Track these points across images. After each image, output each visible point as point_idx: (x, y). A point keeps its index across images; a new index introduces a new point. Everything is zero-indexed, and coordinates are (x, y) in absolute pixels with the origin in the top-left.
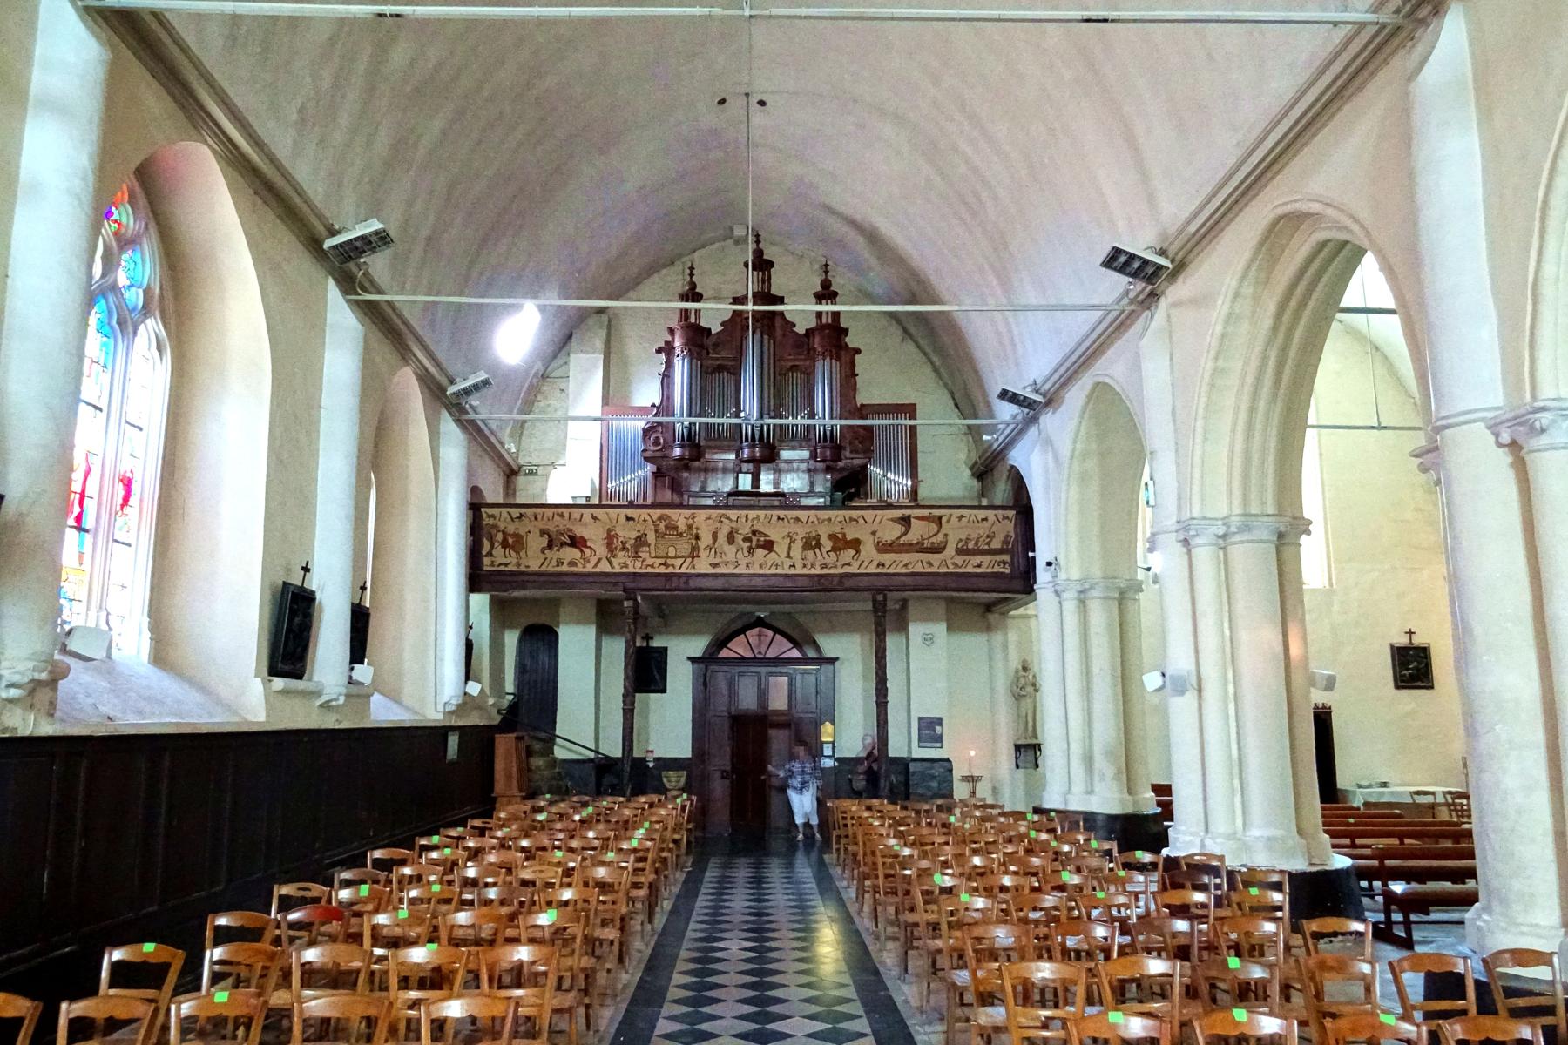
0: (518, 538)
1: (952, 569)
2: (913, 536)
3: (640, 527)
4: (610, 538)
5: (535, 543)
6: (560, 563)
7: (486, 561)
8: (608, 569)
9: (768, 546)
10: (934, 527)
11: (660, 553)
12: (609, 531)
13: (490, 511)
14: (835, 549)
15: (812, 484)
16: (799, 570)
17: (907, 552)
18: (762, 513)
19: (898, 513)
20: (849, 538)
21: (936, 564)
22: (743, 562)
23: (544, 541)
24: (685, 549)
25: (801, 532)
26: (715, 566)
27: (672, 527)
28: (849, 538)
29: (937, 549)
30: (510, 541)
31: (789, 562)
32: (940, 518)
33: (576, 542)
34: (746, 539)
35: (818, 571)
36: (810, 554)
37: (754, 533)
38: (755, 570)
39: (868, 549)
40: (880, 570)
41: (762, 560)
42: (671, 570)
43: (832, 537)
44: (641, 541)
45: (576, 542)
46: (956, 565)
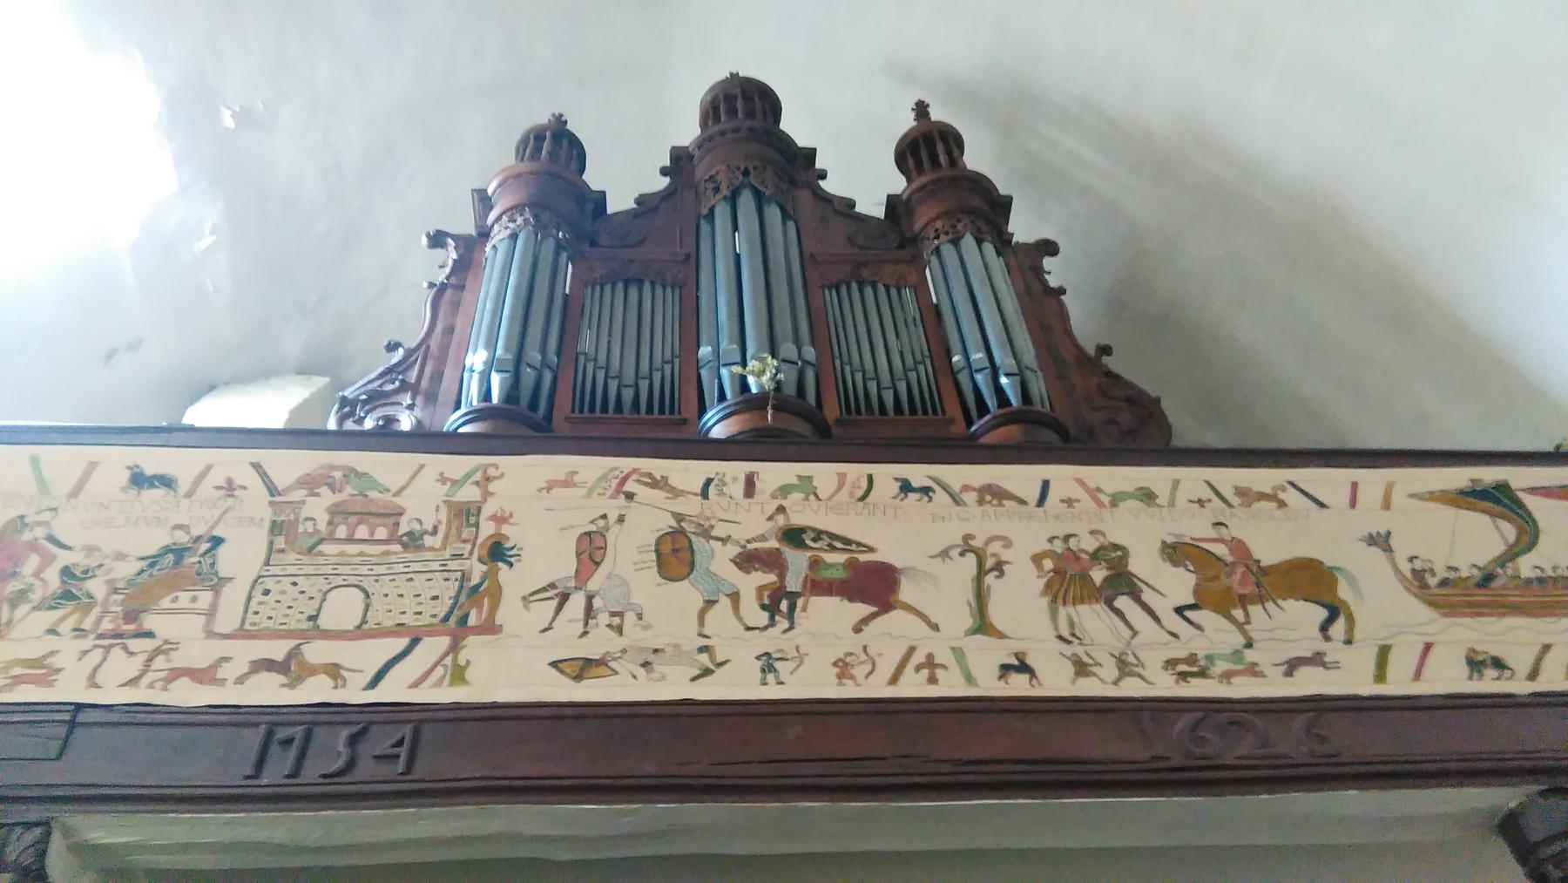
11: (268, 613)
16: (1056, 681)
24: (424, 592)
25: (1026, 537)
26: (584, 668)
34: (747, 561)
35: (1165, 686)
36: (1092, 618)
37: (794, 536)
42: (316, 690)
43: (1176, 552)
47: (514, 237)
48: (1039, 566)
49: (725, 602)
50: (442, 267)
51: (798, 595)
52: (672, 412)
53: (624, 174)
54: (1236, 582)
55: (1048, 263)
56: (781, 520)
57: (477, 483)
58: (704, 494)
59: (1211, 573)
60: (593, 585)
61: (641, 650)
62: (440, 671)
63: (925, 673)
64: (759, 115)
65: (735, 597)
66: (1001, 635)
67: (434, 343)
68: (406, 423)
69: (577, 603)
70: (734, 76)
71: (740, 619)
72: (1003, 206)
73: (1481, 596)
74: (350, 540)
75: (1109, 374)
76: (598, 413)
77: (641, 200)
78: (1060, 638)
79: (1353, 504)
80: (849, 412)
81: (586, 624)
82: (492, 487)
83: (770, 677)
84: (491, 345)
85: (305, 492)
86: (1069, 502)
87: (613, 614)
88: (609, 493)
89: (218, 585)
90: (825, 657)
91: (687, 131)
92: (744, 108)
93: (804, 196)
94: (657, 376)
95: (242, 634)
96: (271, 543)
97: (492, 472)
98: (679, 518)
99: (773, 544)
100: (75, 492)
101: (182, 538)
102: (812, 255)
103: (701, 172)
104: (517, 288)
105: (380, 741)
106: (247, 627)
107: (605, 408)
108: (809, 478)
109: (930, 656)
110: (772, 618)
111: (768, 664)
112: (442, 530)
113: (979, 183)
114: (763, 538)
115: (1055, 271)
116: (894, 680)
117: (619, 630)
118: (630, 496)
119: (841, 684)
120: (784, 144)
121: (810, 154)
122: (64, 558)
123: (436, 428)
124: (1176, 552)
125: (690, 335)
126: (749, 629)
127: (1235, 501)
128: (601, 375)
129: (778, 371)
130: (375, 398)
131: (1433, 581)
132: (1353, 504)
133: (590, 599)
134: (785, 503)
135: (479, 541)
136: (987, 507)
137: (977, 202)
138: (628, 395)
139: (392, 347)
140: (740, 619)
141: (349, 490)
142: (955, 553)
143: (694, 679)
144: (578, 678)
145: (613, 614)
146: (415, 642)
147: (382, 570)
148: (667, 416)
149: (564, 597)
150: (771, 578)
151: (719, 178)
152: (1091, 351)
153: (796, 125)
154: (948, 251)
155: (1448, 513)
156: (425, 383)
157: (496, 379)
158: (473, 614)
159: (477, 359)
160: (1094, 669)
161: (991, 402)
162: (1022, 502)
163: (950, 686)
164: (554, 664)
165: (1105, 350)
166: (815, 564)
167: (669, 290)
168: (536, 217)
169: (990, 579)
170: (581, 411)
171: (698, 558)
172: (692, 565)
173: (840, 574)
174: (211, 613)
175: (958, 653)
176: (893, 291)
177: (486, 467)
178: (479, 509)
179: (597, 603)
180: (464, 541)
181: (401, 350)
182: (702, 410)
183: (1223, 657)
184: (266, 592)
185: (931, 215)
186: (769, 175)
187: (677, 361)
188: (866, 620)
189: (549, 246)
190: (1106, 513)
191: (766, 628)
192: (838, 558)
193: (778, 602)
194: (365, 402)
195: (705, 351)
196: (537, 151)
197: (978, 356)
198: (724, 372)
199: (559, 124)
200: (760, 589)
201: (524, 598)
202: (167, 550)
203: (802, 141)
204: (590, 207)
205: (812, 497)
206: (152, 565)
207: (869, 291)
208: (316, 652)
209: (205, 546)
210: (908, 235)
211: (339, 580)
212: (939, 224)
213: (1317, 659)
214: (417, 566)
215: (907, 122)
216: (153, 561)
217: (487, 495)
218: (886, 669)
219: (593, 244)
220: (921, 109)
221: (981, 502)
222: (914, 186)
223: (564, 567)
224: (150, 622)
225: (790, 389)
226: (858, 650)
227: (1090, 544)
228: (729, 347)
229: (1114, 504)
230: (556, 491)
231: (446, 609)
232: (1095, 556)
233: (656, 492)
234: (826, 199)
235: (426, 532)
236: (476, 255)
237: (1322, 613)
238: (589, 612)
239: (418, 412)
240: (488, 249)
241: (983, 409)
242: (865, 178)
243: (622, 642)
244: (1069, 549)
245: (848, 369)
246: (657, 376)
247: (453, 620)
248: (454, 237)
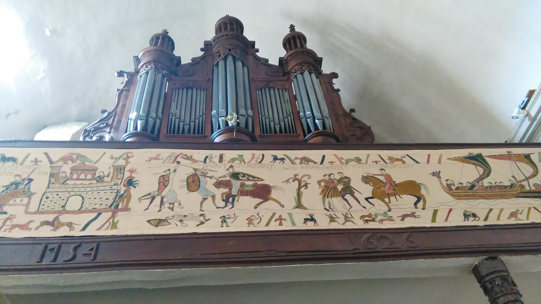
10: (528, 170)
16: (323, 223)
17: (502, 196)
24: (104, 197)
25: (315, 175)
26: (159, 222)
34: (219, 184)
35: (360, 225)
36: (337, 202)
37: (235, 176)
38: (239, 225)
42: (63, 232)
43: (367, 179)
47: (147, 73)
48: (320, 185)
49: (210, 199)
50: (122, 83)
51: (236, 196)
52: (202, 133)
53: (187, 51)
55: (334, 81)
56: (231, 170)
57: (124, 159)
58: (205, 161)
59: (378, 186)
60: (164, 194)
61: (180, 216)
62: (108, 224)
63: (278, 222)
64: (235, 30)
65: (213, 197)
66: (305, 209)
67: (119, 110)
68: (107, 138)
69: (158, 200)
70: (227, 16)
71: (215, 205)
72: (319, 61)
74: (78, 179)
75: (354, 119)
76: (176, 134)
77: (193, 60)
78: (326, 209)
79: (428, 162)
80: (263, 133)
81: (161, 207)
82: (129, 160)
83: (224, 224)
84: (138, 110)
85: (63, 163)
86: (331, 163)
87: (170, 204)
88: (171, 162)
89: (30, 195)
90: (245, 217)
91: (210, 35)
92: (231, 28)
93: (251, 58)
94: (197, 121)
95: (38, 212)
96: (50, 181)
97: (130, 155)
98: (196, 170)
99: (228, 178)
101: (18, 179)
102: (253, 78)
103: (214, 50)
104: (148, 90)
105: (85, 249)
106: (40, 210)
107: (178, 133)
108: (242, 156)
109: (280, 216)
110: (226, 204)
111: (224, 220)
112: (111, 175)
113: (311, 54)
114: (225, 176)
115: (337, 83)
116: (267, 224)
117: (172, 209)
118: (178, 163)
119: (249, 226)
120: (244, 40)
121: (253, 44)
123: (118, 140)
125: (209, 106)
126: (218, 208)
127: (388, 161)
128: (177, 121)
129: (238, 118)
130: (97, 130)
131: (454, 188)
132: (428, 162)
133: (162, 199)
134: (233, 164)
135: (124, 179)
136: (303, 165)
137: (310, 60)
138: (187, 127)
139: (103, 112)
140: (215, 205)
141: (78, 162)
142: (291, 181)
143: (197, 226)
144: (157, 226)
145: (170, 204)
146: (99, 214)
147: (89, 189)
148: (200, 135)
149: (153, 198)
150: (227, 190)
151: (220, 52)
152: (348, 111)
153: (249, 34)
154: (299, 77)
155: (461, 164)
156: (115, 124)
157: (139, 122)
158: (121, 204)
159: (133, 115)
160: (336, 219)
161: (312, 129)
162: (316, 163)
163: (287, 226)
164: (148, 221)
165: (352, 110)
166: (242, 185)
167: (202, 91)
168: (155, 65)
169: (303, 189)
170: (170, 133)
171: (201, 183)
172: (199, 186)
173: (251, 189)
176: (280, 90)
177: (128, 153)
178: (125, 168)
179: (165, 200)
180: (119, 179)
181: (107, 113)
182: (212, 132)
183: (380, 215)
184: (47, 198)
185: (294, 64)
186: (238, 50)
187: (204, 116)
188: (259, 204)
189: (160, 75)
190: (344, 166)
191: (224, 207)
193: (229, 199)
194: (93, 131)
195: (214, 112)
196: (156, 43)
197: (308, 113)
198: (220, 119)
199: (166, 33)
200: (223, 194)
201: (139, 199)
202: (12, 184)
203: (250, 39)
204: (175, 62)
205: (243, 162)
206: (7, 189)
207: (272, 91)
208: (64, 218)
209: (26, 182)
210: (286, 71)
211: (73, 193)
212: (296, 67)
213: (413, 215)
214: (102, 188)
215: (287, 31)
216: (7, 187)
217: (127, 163)
218: (265, 221)
219: (176, 75)
220: (292, 27)
221: (301, 163)
222: (289, 54)
223: (154, 187)
225: (243, 125)
226: (256, 215)
227: (338, 177)
228: (222, 111)
229: (347, 163)
230: (152, 161)
231: (111, 203)
232: (339, 181)
233: (188, 161)
234: (258, 59)
235: (105, 176)
236: (134, 78)
237: (416, 199)
238: (162, 202)
239: (112, 134)
240: (138, 77)
241: (310, 131)
242: (272, 51)
243: (173, 213)
244: (330, 179)
245: (264, 118)
246: (197, 121)
247: (113, 207)
248: (127, 73)
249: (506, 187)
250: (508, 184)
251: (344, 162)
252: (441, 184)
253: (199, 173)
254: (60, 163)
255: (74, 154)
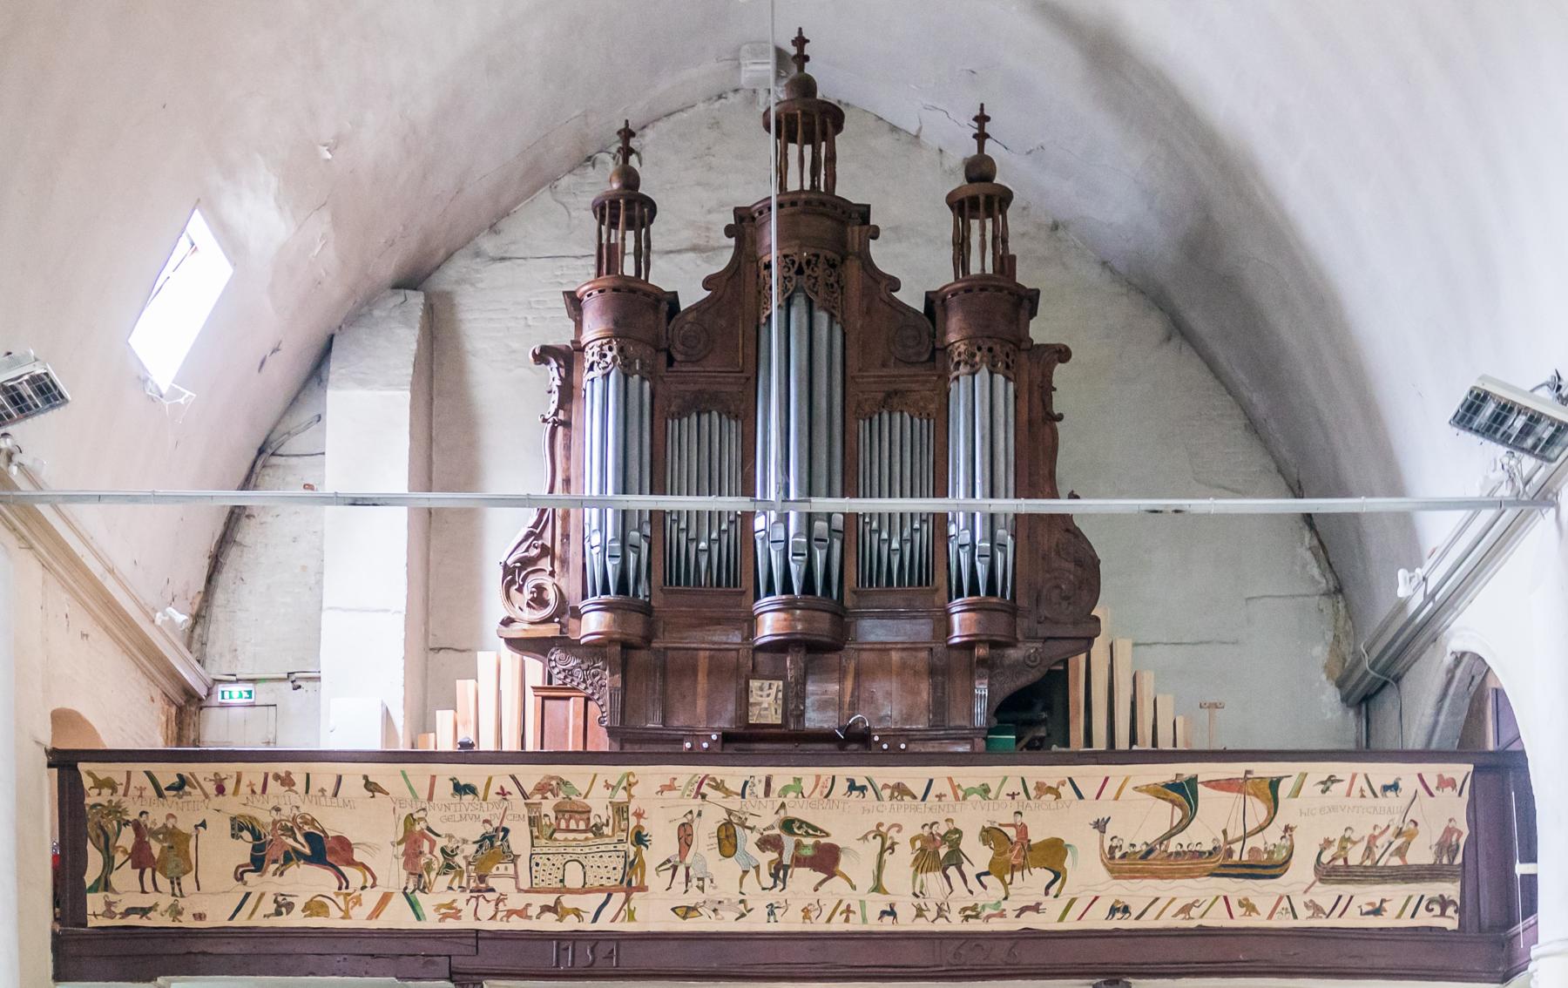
0: (176, 840)
1: (1305, 920)
2: (1200, 835)
3: (491, 811)
4: (413, 840)
5: (220, 853)
6: (283, 906)
7: (95, 903)
8: (407, 921)
9: (826, 860)
12: (410, 820)
13: (103, 770)
14: (1001, 869)
15: (939, 707)
16: (906, 922)
17: (1188, 874)
18: (808, 774)
19: (1166, 772)
20: (1035, 837)
21: (1264, 906)
22: (759, 904)
23: (242, 850)
24: (608, 868)
25: (910, 822)
26: (687, 912)
27: (572, 811)
28: (1035, 837)
29: (1266, 868)
30: (156, 848)
31: (878, 903)
32: (1274, 784)
33: (324, 850)
34: (766, 843)
35: (956, 924)
36: (934, 880)
37: (788, 825)
38: (789, 922)
39: (1086, 868)
40: (1119, 923)
41: (812, 898)
42: (570, 924)
43: (990, 835)
44: (493, 844)
45: (324, 850)
46: (1317, 910)
48: (913, 846)
49: (753, 872)
51: (788, 867)
54: (1013, 857)
60: (688, 860)
65: (757, 868)
66: (886, 893)
69: (681, 870)
73: (1140, 865)
74: (568, 830)
82: (634, 791)
86: (940, 797)
97: (632, 780)
98: (729, 812)
99: (777, 831)
100: (430, 798)
105: (603, 949)
114: (772, 827)
116: (829, 920)
117: (702, 889)
118: (704, 796)
122: (441, 843)
124: (990, 835)
127: (1032, 793)
131: (1118, 854)
141: (562, 795)
142: (870, 837)
144: (684, 918)
146: (610, 895)
147: (586, 850)
149: (675, 868)
150: (776, 855)
163: (855, 925)
166: (798, 845)
169: (886, 855)
173: (808, 852)
174: (516, 877)
175: (862, 903)
177: (629, 774)
179: (691, 872)
192: (809, 841)
193: (779, 872)
200: (771, 862)
202: (484, 838)
208: (568, 901)
211: (568, 857)
213: (1036, 908)
214: (602, 848)
216: (480, 843)
221: (892, 797)
223: (672, 849)
224: (491, 882)
229: (964, 798)
230: (666, 793)
232: (944, 838)
237: (1052, 876)
249: (1201, 853)
250: (1207, 847)
251: (961, 793)
252: (1102, 846)
253: (735, 820)
254: (537, 798)
255: (552, 778)
